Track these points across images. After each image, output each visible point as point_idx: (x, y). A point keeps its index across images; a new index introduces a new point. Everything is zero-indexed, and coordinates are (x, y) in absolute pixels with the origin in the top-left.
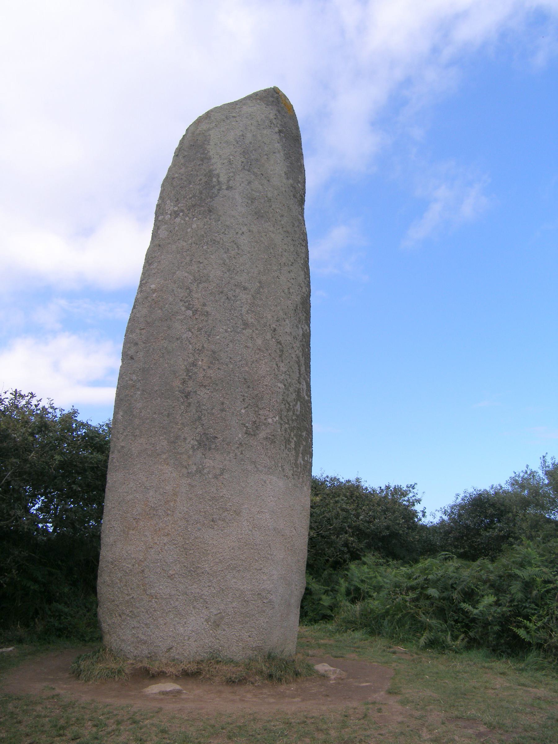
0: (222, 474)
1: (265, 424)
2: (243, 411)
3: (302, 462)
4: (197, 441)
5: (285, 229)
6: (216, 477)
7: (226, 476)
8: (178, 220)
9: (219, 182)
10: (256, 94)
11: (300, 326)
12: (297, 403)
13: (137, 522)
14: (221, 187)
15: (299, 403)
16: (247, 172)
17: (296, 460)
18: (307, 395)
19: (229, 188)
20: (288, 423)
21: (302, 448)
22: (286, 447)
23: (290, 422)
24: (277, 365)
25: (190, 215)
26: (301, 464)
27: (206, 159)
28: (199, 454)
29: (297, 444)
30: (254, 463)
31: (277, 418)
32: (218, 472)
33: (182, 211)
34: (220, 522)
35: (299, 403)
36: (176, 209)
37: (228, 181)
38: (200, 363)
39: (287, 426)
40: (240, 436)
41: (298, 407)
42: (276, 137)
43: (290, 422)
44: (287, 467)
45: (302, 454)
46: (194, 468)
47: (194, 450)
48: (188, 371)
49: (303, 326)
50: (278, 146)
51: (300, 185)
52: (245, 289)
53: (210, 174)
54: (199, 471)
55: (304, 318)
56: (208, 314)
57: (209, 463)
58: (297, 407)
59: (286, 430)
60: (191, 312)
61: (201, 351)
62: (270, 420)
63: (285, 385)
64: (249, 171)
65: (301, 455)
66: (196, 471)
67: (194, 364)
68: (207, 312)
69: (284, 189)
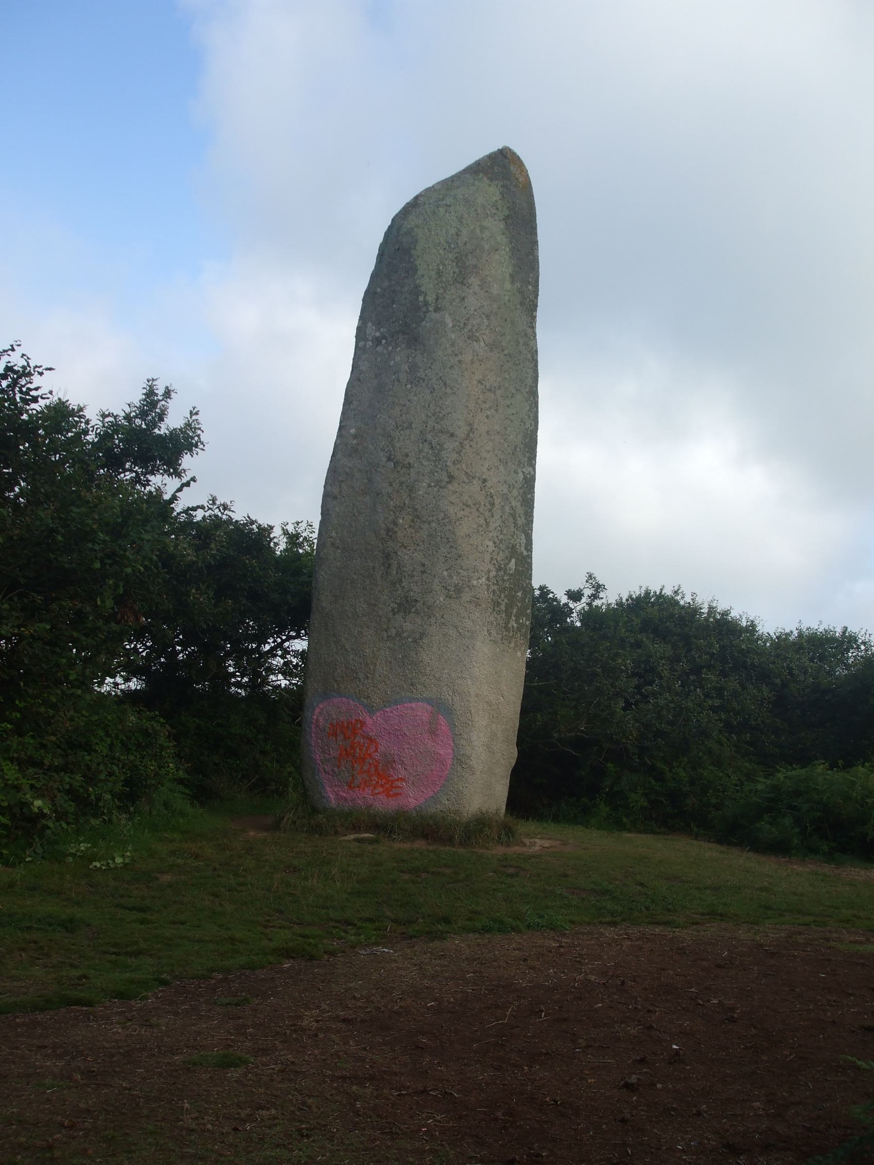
0: (421, 638)
1: (469, 587)
2: (445, 573)
3: (515, 625)
4: (397, 604)
5: (506, 352)
6: (415, 641)
7: (426, 640)
8: (379, 349)
9: (426, 304)
10: (478, 164)
11: (519, 471)
12: (510, 561)
13: (338, 685)
14: (427, 309)
15: (513, 561)
16: (459, 286)
17: (507, 623)
18: (526, 549)
19: (437, 309)
20: (497, 584)
21: (515, 611)
22: (494, 610)
23: (500, 583)
24: (485, 520)
25: (393, 344)
26: (513, 627)
27: (412, 270)
28: (399, 617)
29: (509, 607)
30: (456, 627)
31: (484, 580)
32: (418, 636)
33: (385, 337)
34: (419, 686)
35: (513, 561)
36: (378, 334)
37: (437, 299)
38: (401, 521)
39: (496, 587)
40: (442, 599)
41: (512, 564)
42: (502, 226)
43: (500, 583)
44: (494, 632)
45: (516, 616)
46: (394, 631)
47: (394, 614)
48: (388, 530)
49: (524, 470)
50: (502, 239)
51: (530, 287)
52: (452, 435)
53: (416, 291)
54: (398, 634)
55: (526, 459)
56: (409, 466)
57: (408, 626)
58: (510, 565)
59: (494, 591)
60: (392, 464)
61: (402, 508)
62: (475, 583)
63: (495, 543)
64: (462, 283)
65: (514, 618)
66: (396, 635)
67: (395, 524)
68: (409, 464)
69: (507, 298)
